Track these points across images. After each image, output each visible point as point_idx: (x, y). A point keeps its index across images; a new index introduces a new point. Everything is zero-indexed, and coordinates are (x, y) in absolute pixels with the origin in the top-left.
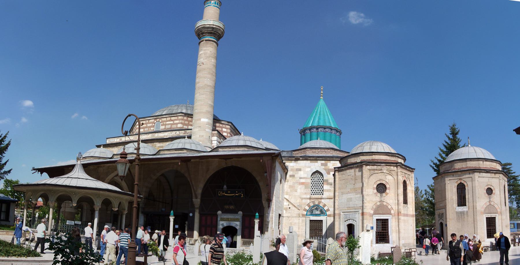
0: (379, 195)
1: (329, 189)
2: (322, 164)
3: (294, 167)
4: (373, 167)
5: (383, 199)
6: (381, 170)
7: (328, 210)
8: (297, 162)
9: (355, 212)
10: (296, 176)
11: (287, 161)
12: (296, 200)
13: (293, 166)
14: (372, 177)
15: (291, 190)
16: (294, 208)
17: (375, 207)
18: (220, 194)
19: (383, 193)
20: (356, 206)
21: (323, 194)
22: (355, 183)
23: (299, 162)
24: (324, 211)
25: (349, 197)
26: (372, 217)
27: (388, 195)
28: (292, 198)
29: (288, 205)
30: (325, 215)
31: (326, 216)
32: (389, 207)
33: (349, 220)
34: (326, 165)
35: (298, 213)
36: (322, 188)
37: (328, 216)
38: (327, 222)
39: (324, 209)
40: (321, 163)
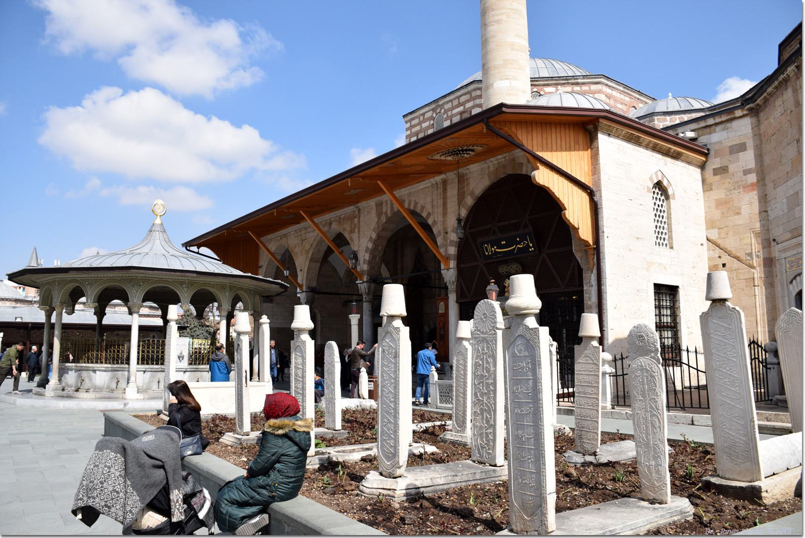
3: (724, 145)
8: (732, 128)
10: (732, 168)
11: (700, 132)
12: (741, 240)
13: (720, 142)
15: (723, 213)
16: (736, 264)
18: (487, 251)
23: (735, 124)
28: (727, 234)
29: (720, 257)
33: (798, 278)
35: (750, 276)
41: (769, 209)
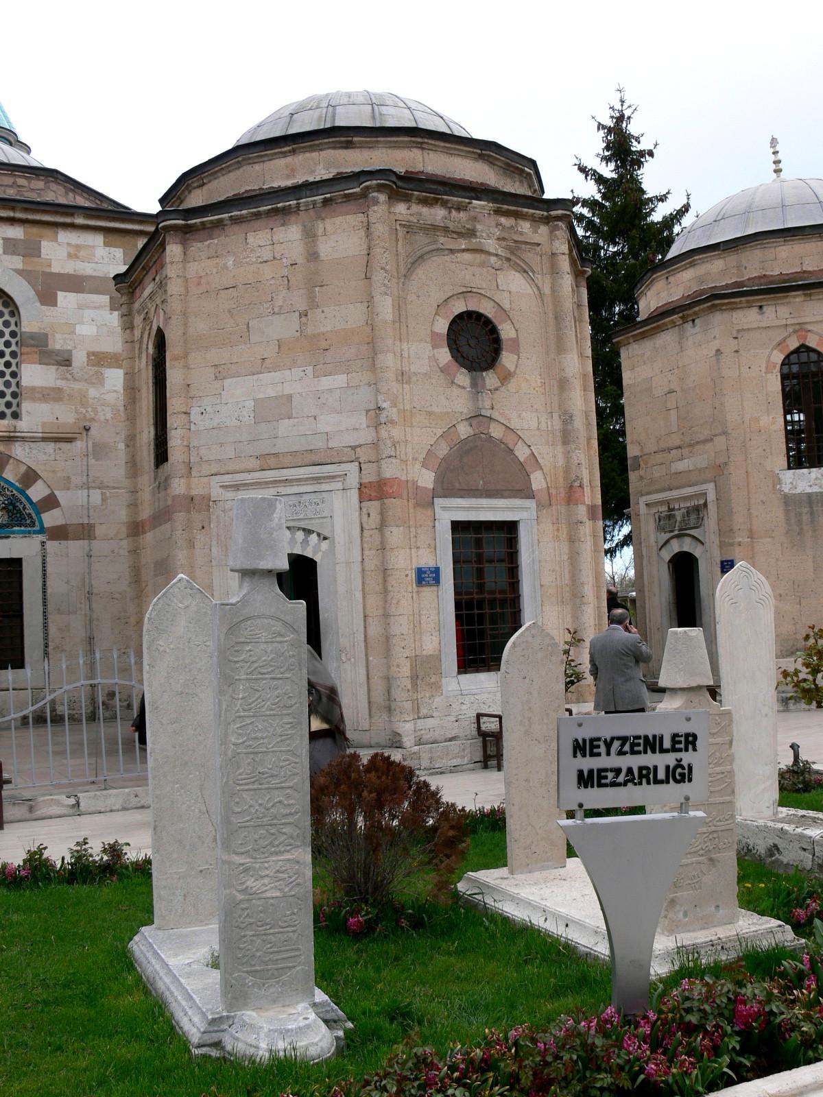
0: (463, 377)
1: (51, 384)
2: (11, 247)
4: (425, 210)
5: (487, 404)
6: (472, 233)
7: (50, 502)
9: (317, 480)
14: (420, 272)
17: (443, 450)
19: (486, 369)
20: (321, 444)
21: (16, 416)
22: (313, 303)
24: (30, 510)
25: (271, 392)
26: (429, 512)
27: (512, 385)
30: (35, 533)
31: (41, 538)
32: (521, 453)
34: (30, 250)
36: (13, 381)
37: (51, 538)
38: (49, 569)
39: (28, 498)
40: (6, 240)
41: (195, 412)
